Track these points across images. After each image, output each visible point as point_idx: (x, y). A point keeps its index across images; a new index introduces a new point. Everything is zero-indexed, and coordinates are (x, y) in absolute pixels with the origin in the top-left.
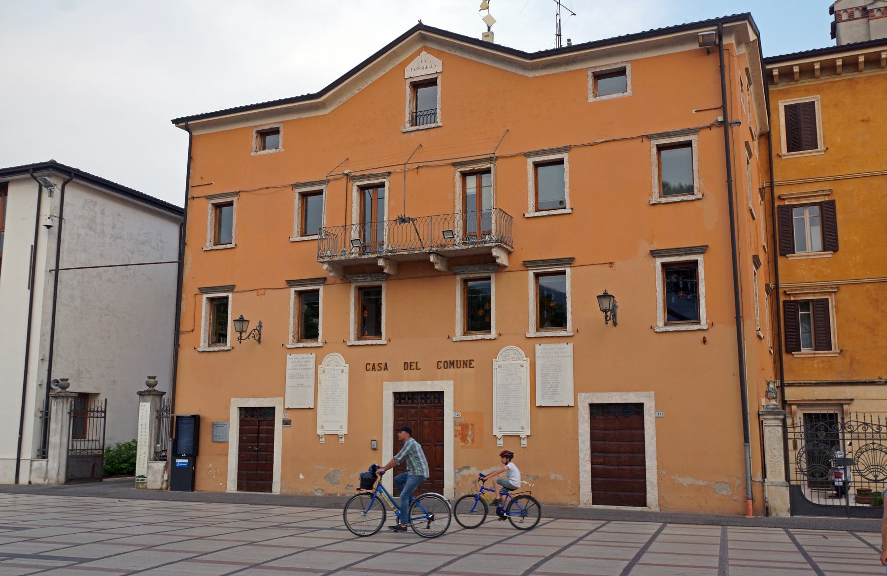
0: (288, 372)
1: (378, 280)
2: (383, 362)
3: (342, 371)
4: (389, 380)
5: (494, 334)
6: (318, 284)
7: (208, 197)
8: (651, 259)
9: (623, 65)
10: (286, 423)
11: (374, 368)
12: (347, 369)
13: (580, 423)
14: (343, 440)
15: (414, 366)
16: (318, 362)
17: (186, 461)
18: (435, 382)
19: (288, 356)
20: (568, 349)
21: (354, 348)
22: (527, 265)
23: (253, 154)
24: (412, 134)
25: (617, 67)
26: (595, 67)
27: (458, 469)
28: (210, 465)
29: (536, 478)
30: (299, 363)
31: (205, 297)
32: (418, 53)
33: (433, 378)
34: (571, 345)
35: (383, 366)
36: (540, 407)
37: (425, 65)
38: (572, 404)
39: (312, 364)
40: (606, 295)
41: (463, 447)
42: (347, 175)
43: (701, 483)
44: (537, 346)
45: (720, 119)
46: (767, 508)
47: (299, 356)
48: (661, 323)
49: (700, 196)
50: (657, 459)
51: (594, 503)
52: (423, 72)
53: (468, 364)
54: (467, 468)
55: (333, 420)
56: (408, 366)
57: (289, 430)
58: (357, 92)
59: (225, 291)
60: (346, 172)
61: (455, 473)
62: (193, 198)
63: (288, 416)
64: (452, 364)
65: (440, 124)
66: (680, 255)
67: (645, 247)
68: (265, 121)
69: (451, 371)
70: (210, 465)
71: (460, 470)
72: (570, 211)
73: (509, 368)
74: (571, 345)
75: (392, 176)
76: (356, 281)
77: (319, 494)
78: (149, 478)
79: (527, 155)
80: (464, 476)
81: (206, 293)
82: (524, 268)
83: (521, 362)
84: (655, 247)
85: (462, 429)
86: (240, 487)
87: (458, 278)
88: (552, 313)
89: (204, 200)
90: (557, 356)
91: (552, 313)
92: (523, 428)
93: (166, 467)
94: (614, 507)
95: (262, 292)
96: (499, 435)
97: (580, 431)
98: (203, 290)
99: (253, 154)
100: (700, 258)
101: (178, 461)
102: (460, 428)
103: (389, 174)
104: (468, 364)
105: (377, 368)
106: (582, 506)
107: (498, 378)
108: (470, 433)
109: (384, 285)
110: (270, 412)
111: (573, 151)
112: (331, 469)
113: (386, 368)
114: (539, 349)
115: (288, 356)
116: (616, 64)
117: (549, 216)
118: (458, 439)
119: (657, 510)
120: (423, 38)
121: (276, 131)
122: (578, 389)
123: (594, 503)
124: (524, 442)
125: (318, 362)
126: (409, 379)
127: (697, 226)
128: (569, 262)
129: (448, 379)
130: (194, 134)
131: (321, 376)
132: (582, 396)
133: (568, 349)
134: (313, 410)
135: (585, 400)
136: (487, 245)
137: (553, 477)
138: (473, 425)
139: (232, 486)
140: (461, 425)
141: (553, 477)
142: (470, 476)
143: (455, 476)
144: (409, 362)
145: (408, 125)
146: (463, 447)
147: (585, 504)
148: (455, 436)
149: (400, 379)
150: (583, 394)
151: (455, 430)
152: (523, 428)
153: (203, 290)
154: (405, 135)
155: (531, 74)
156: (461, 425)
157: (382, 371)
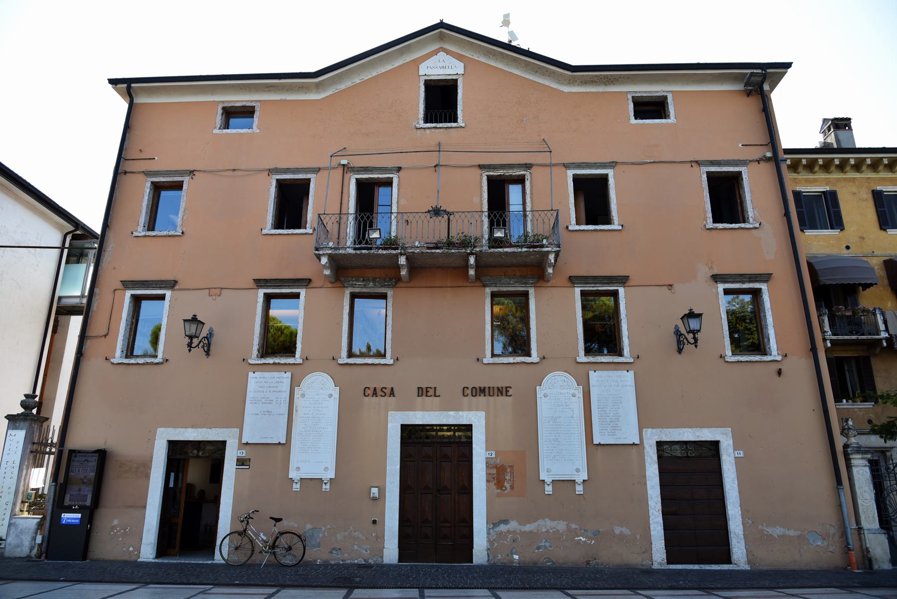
0: (250, 395)
2: (389, 386)
3: (331, 396)
5: (535, 357)
7: (148, 174)
8: (712, 283)
9: (665, 94)
10: (241, 462)
11: (375, 394)
13: (647, 465)
14: (328, 486)
15: (431, 392)
16: (295, 383)
17: (79, 516)
18: (461, 413)
19: (251, 374)
20: (628, 377)
21: (347, 368)
22: (574, 280)
23: (216, 131)
24: (428, 131)
26: (636, 92)
27: (493, 522)
28: (116, 522)
29: (597, 533)
30: (265, 385)
32: (435, 53)
33: (458, 408)
34: (631, 373)
35: (388, 391)
36: (600, 444)
37: (441, 66)
38: (637, 442)
41: (498, 495)
42: (344, 165)
43: (792, 533)
44: (591, 373)
45: (769, 154)
46: (870, 560)
47: (266, 374)
48: (729, 352)
49: (757, 225)
50: (741, 506)
51: (669, 563)
52: (441, 72)
53: (503, 391)
54: (506, 522)
56: (423, 392)
57: (246, 472)
58: (358, 81)
59: (161, 288)
61: (488, 530)
62: (126, 173)
63: (243, 454)
64: (482, 391)
65: (463, 125)
66: (743, 282)
67: (704, 272)
68: (237, 100)
69: (482, 399)
70: (116, 522)
71: (495, 525)
72: (620, 228)
74: (631, 373)
75: (402, 173)
76: (353, 286)
78: (9, 540)
79: (567, 166)
80: (501, 533)
81: (133, 288)
82: (570, 284)
83: (573, 391)
84: (716, 271)
85: (498, 473)
87: (488, 290)
88: (602, 336)
89: (142, 176)
91: (602, 336)
92: (578, 470)
93: (40, 525)
94: (696, 567)
95: (218, 291)
96: (548, 480)
97: (648, 473)
99: (216, 131)
101: (65, 516)
102: (494, 471)
103: (399, 169)
104: (503, 391)
105: (379, 393)
106: (656, 566)
111: (618, 167)
112: (309, 526)
113: (392, 393)
114: (595, 377)
115: (251, 374)
116: (657, 92)
117: (596, 230)
118: (492, 484)
119: (748, 568)
120: (441, 38)
121: (247, 112)
122: (642, 424)
123: (669, 563)
124: (579, 489)
125: (295, 383)
126: (424, 409)
128: (623, 280)
129: (477, 410)
130: (138, 100)
133: (628, 377)
134: (285, 446)
135: (652, 437)
136: (546, 249)
137: (617, 530)
138: (511, 467)
139: (147, 552)
140: (496, 467)
141: (617, 530)
142: (509, 532)
143: (488, 534)
144: (424, 386)
145: (422, 122)
146: (498, 495)
147: (660, 564)
148: (488, 481)
149: (412, 408)
150: (650, 430)
151: (488, 474)
152: (578, 470)
154: (419, 131)
155: (566, 89)
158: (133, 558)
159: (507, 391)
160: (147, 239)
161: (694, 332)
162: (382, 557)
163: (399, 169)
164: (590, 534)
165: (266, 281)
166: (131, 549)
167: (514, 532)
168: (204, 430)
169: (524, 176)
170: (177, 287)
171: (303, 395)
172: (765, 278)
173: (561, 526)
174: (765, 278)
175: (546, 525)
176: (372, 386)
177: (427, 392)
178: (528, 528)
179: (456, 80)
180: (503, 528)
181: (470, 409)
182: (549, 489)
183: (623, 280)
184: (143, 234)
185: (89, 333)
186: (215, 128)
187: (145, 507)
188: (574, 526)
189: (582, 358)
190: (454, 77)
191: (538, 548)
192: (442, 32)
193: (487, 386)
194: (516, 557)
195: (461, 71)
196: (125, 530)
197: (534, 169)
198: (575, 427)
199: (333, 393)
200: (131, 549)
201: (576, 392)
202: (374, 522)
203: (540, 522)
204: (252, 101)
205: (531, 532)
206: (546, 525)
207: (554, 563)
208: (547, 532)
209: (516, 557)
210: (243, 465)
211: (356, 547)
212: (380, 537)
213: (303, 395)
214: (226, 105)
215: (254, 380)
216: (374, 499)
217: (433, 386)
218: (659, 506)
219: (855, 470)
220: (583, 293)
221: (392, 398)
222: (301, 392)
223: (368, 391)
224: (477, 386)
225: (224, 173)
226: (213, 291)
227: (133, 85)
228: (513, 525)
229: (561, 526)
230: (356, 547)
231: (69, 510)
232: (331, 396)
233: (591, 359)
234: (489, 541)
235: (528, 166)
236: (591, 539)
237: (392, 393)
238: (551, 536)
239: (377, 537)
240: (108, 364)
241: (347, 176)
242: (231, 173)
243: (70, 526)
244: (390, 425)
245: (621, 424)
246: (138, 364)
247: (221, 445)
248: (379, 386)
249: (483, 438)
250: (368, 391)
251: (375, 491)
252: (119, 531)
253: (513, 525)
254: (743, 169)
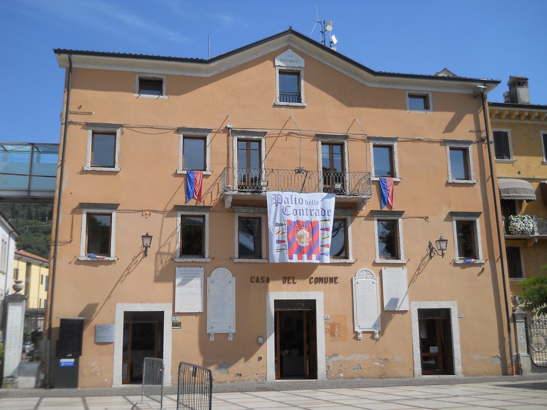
2: (266, 276)
3: (230, 282)
6: (204, 211)
9: (427, 93)
10: (176, 325)
11: (258, 281)
16: (207, 275)
18: (309, 293)
19: (177, 268)
26: (410, 90)
27: (329, 356)
28: (94, 364)
32: (285, 49)
35: (265, 279)
40: (147, 236)
47: (188, 269)
53: (333, 280)
54: (336, 355)
57: (178, 330)
59: (108, 208)
61: (326, 360)
69: (320, 285)
71: (330, 357)
85: (331, 327)
95: (148, 213)
96: (359, 331)
102: (329, 327)
104: (333, 280)
105: (260, 280)
108: (337, 330)
115: (177, 268)
116: (423, 91)
118: (328, 335)
127: (470, 200)
132: (413, 303)
138: (339, 324)
140: (330, 324)
142: (338, 361)
143: (326, 362)
145: (278, 100)
148: (325, 332)
151: (326, 328)
156: (330, 324)
159: (335, 280)
161: (442, 250)
166: (106, 380)
176: (256, 276)
179: (300, 71)
180: (334, 359)
181: (314, 290)
184: (91, 169)
187: (113, 354)
188: (373, 357)
190: (298, 69)
195: (303, 65)
204: (160, 74)
213: (212, 282)
219: (517, 324)
223: (253, 280)
229: (366, 357)
236: (382, 364)
239: (263, 366)
247: (160, 315)
253: (340, 357)
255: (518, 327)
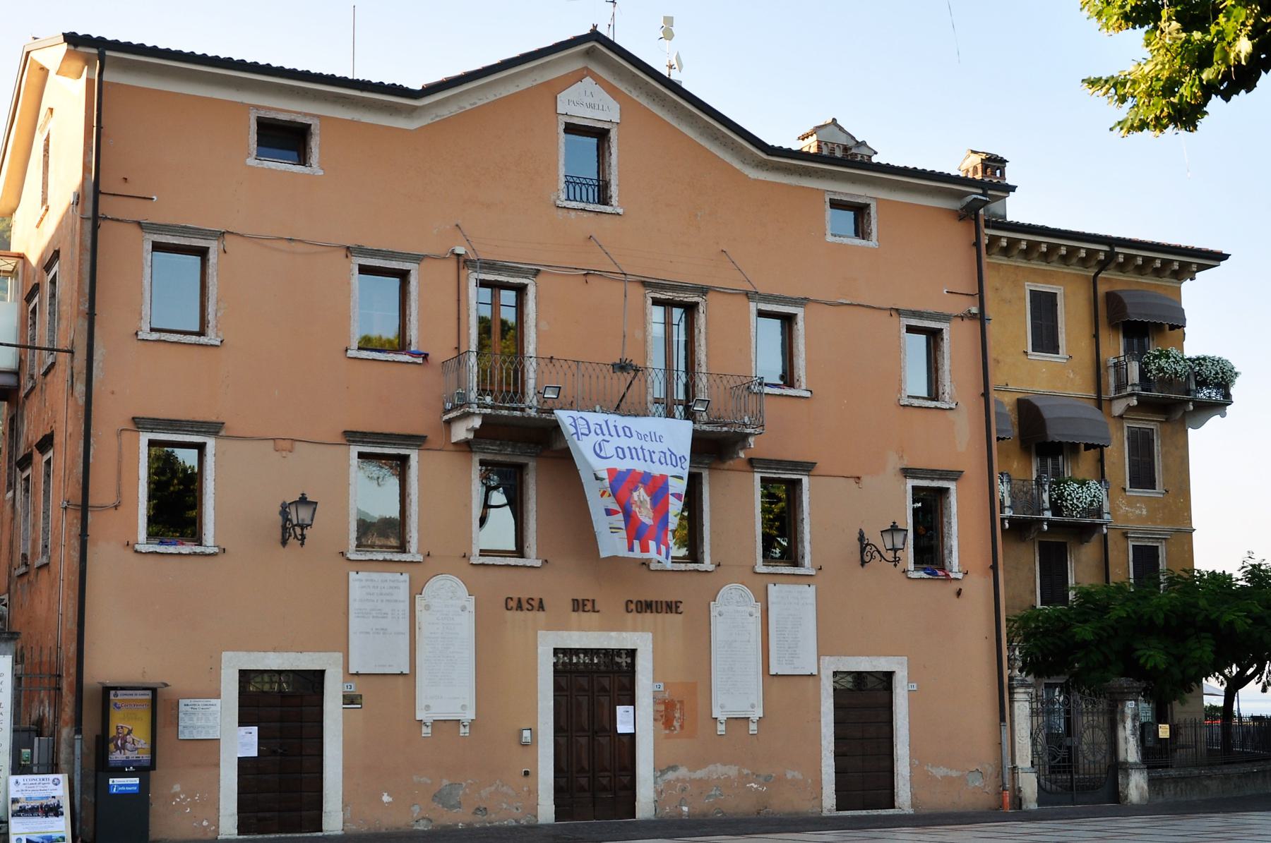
0: (354, 606)
1: (523, 454)
2: (536, 596)
3: (463, 609)
4: (549, 628)
5: (707, 565)
6: (408, 446)
8: (901, 477)
11: (520, 607)
12: (471, 603)
15: (589, 607)
16: (415, 590)
17: (136, 781)
18: (624, 634)
19: (352, 575)
21: (482, 569)
24: (573, 213)
25: (859, 201)
27: (661, 770)
28: (177, 788)
29: (767, 779)
30: (373, 593)
31: (145, 438)
32: (578, 77)
33: (621, 628)
34: (813, 588)
36: (776, 675)
37: (589, 101)
39: (403, 593)
41: (667, 737)
42: (458, 255)
43: (954, 774)
44: (771, 587)
45: (975, 310)
47: (375, 576)
48: (911, 566)
49: (953, 406)
52: (589, 113)
54: (673, 768)
55: (447, 693)
57: (356, 712)
58: (469, 107)
59: (198, 433)
60: (460, 250)
61: (656, 778)
63: (353, 688)
65: (620, 211)
66: (932, 479)
67: (894, 463)
69: (648, 617)
70: (177, 788)
71: (663, 772)
72: (808, 394)
73: (732, 613)
74: (813, 588)
75: (540, 278)
76: (482, 451)
77: (422, 826)
82: (748, 468)
83: (750, 609)
84: (906, 463)
85: (666, 709)
86: (242, 828)
89: (135, 230)
90: (795, 603)
92: (753, 706)
94: (864, 813)
95: (287, 444)
96: (722, 718)
98: (140, 423)
100: (952, 486)
101: (115, 782)
102: (662, 708)
103: (537, 273)
105: (525, 605)
106: (825, 813)
107: (720, 631)
108: (677, 715)
109: (532, 464)
110: (316, 678)
112: (445, 782)
113: (541, 607)
115: (352, 575)
117: (781, 395)
118: (660, 724)
119: (911, 811)
120: (589, 53)
123: (838, 809)
124: (753, 728)
125: (415, 590)
126: (580, 628)
128: (807, 467)
129: (643, 630)
131: (421, 615)
132: (826, 660)
133: (808, 593)
134: (409, 677)
136: (748, 431)
137: (789, 776)
138: (681, 702)
140: (664, 702)
141: (789, 776)
142: (678, 780)
144: (580, 598)
146: (667, 737)
147: (829, 810)
148: (655, 720)
149: (565, 627)
151: (656, 711)
152: (753, 706)
153: (140, 423)
154: (560, 212)
155: (753, 174)
156: (664, 702)
157: (534, 613)
158: (210, 836)
159: (677, 607)
160: (162, 346)
161: (895, 550)
162: (536, 816)
163: (537, 273)
164: (761, 780)
165: (364, 434)
166: (205, 823)
167: (684, 781)
168: (293, 655)
169: (697, 304)
170: (223, 433)
171: (427, 607)
172: (954, 475)
173: (732, 771)
174: (954, 475)
175: (718, 771)
176: (515, 596)
177: (584, 605)
178: (700, 774)
179: (608, 131)
180: (671, 775)
181: (635, 630)
182: (721, 729)
183: (807, 467)
185: (92, 501)
186: (249, 155)
187: (218, 765)
188: (745, 771)
189: (760, 568)
190: (606, 126)
191: (709, 797)
192: (595, 47)
193: (654, 599)
194: (685, 809)
195: (616, 119)
196: (193, 797)
197: (711, 296)
198: (753, 654)
199: (466, 604)
200: (205, 823)
201: (754, 610)
202: (526, 773)
203: (711, 767)
204: (306, 115)
205: (701, 779)
206: (718, 771)
207: (724, 814)
208: (718, 778)
209: (685, 809)
210: (352, 703)
211: (505, 806)
212: (533, 792)
213: (427, 607)
214: (263, 114)
215: (359, 583)
216: (525, 745)
217: (590, 598)
218: (832, 747)
219: (1016, 705)
220: (763, 479)
221: (541, 613)
222: (424, 603)
223: (511, 604)
224: (642, 599)
225: (266, 242)
226: (281, 444)
227: (108, 53)
228: (683, 772)
229: (732, 771)
230: (505, 806)
231: (120, 771)
232: (463, 609)
233: (771, 570)
234: (656, 791)
235: (703, 290)
236: (762, 785)
237: (541, 607)
238: (722, 781)
239: (529, 792)
240: (129, 553)
241: (463, 273)
242: (283, 245)
243: (124, 796)
244: (540, 650)
245: (800, 652)
246: (180, 554)
247: (316, 678)
248: (524, 596)
249: (650, 666)
250: (511, 604)
251: (527, 734)
252: (184, 800)
253: (683, 772)
254: (944, 326)
255: (1017, 711)
